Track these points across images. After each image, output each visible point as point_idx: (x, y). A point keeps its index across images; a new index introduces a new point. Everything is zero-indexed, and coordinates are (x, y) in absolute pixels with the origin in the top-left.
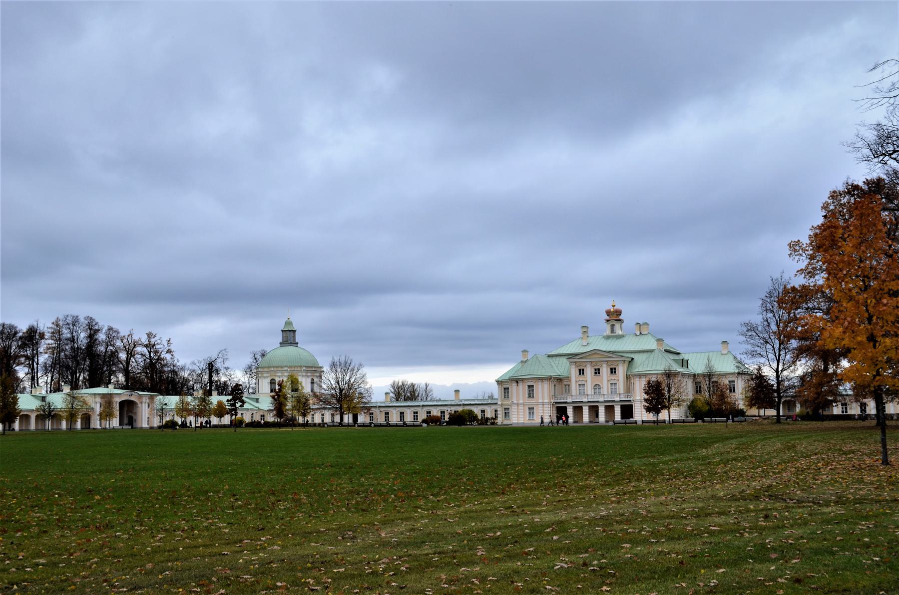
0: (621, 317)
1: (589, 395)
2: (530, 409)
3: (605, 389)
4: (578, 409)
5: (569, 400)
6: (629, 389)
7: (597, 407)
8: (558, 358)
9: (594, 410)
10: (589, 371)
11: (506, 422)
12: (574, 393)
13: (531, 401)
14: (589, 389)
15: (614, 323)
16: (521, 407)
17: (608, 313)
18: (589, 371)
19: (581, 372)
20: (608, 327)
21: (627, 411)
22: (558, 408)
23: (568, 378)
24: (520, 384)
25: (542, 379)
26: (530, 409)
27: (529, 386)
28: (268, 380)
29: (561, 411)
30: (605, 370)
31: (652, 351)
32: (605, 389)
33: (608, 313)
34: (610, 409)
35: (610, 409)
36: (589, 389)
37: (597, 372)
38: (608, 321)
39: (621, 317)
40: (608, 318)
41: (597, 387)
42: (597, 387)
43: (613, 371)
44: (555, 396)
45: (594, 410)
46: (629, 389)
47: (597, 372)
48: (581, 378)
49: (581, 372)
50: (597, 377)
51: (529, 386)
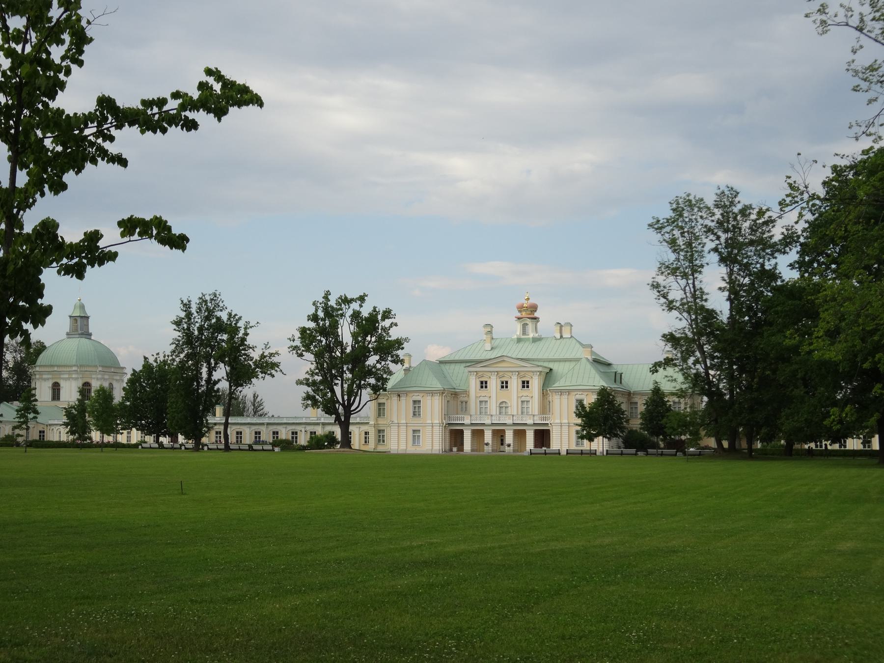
0: (536, 315)
1: (491, 417)
2: (414, 431)
3: (514, 408)
5: (467, 421)
6: (545, 408)
7: (504, 431)
8: (453, 366)
10: (494, 384)
11: (381, 448)
12: (473, 412)
13: (416, 420)
14: (493, 407)
15: (528, 321)
16: (403, 428)
17: (521, 308)
18: (494, 384)
19: (484, 385)
20: (518, 327)
21: (543, 437)
22: (452, 431)
23: (466, 393)
24: (403, 398)
25: (432, 393)
26: (414, 431)
27: (415, 402)
28: (49, 384)
29: (456, 437)
30: (515, 384)
31: (578, 360)
32: (514, 408)
33: (521, 308)
34: (520, 434)
35: (520, 434)
36: (493, 407)
37: (505, 385)
38: (519, 318)
39: (536, 315)
40: (519, 315)
41: (503, 406)
42: (503, 406)
43: (525, 384)
45: (499, 435)
46: (545, 408)
47: (505, 385)
48: (484, 392)
49: (484, 385)
51: (415, 402)
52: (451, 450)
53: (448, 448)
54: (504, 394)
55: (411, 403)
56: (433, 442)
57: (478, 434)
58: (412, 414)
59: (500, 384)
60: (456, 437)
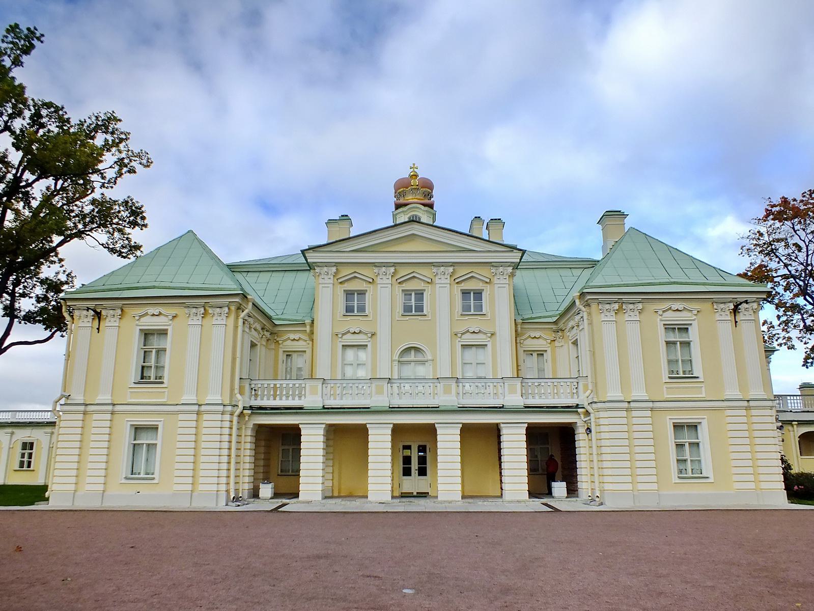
4: (347, 439)
5: (309, 401)
7: (431, 430)
9: (415, 450)
13: (148, 394)
16: (100, 421)
18: (384, 298)
24: (110, 322)
26: (138, 430)
27: (147, 335)
34: (482, 439)
37: (414, 305)
44: (247, 382)
47: (414, 305)
48: (354, 323)
49: (354, 304)
50: (413, 322)
51: (147, 335)
52: (255, 494)
53: (246, 487)
54: (413, 331)
55: (136, 340)
56: (202, 471)
57: (347, 439)
58: (134, 374)
59: (400, 299)
60: (277, 447)
